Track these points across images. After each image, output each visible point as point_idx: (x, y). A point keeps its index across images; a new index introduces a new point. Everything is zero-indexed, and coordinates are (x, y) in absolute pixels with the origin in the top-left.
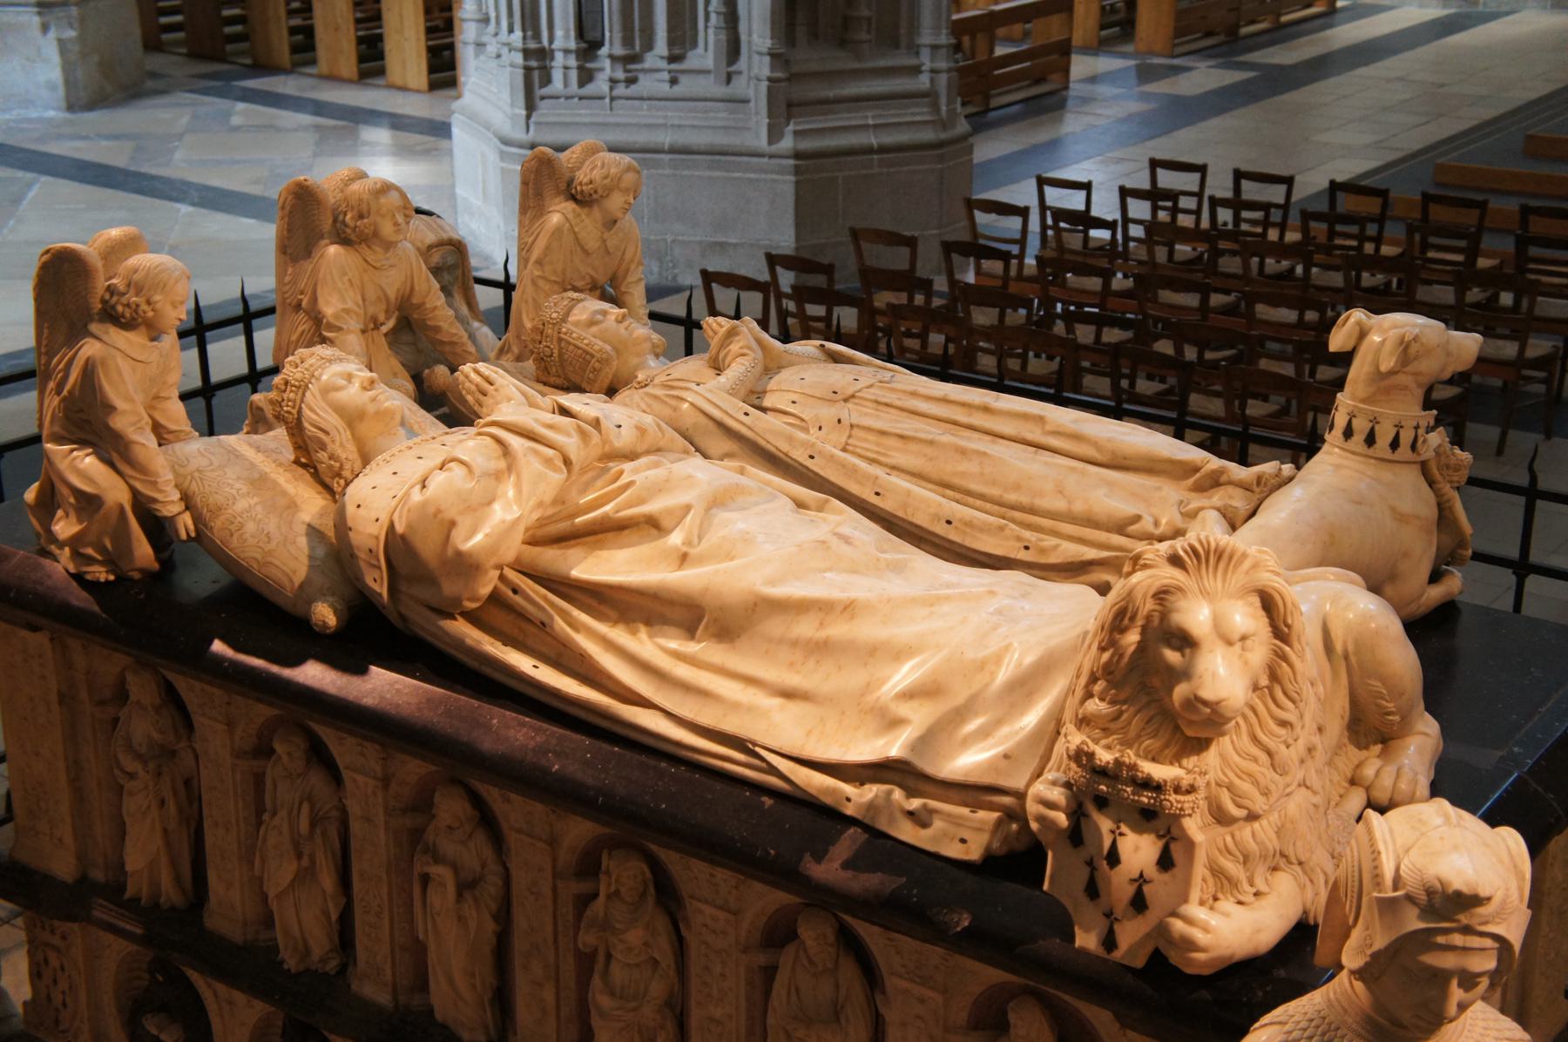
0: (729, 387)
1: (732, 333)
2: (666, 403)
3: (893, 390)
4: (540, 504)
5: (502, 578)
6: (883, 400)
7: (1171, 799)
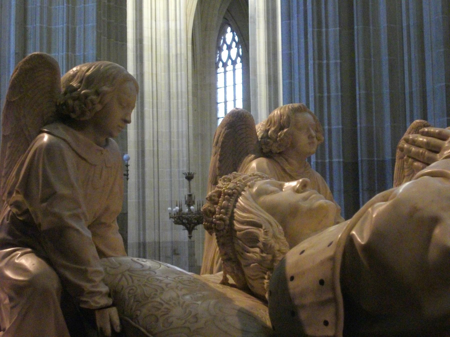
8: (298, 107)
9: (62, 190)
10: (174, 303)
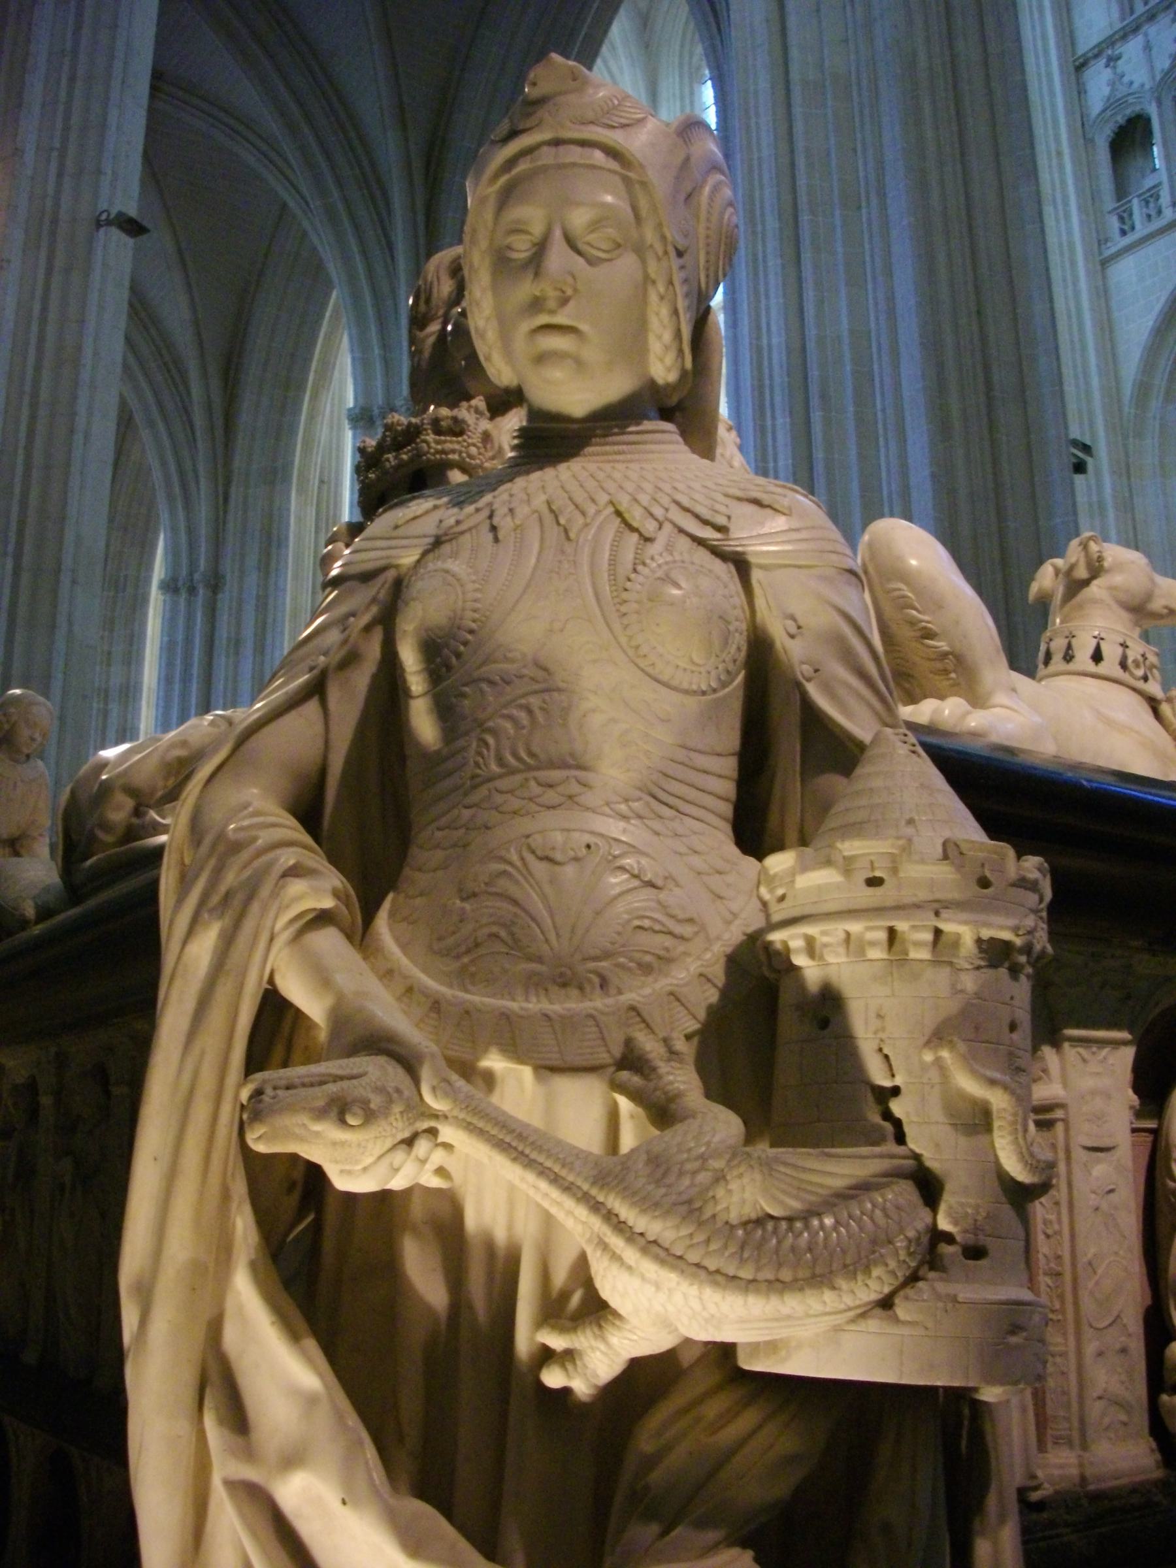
7: (428, 438)
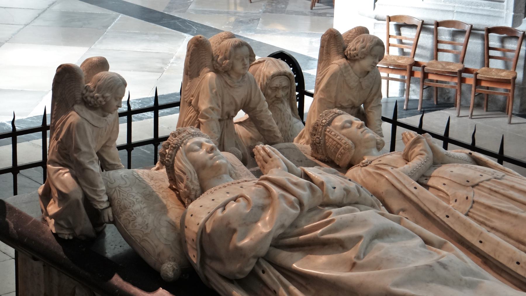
0: (409, 172)
1: (416, 142)
2: (373, 176)
3: (501, 184)
4: (282, 226)
5: (258, 263)
6: (494, 189)
8: (238, 45)
9: (84, 148)
10: (139, 214)
